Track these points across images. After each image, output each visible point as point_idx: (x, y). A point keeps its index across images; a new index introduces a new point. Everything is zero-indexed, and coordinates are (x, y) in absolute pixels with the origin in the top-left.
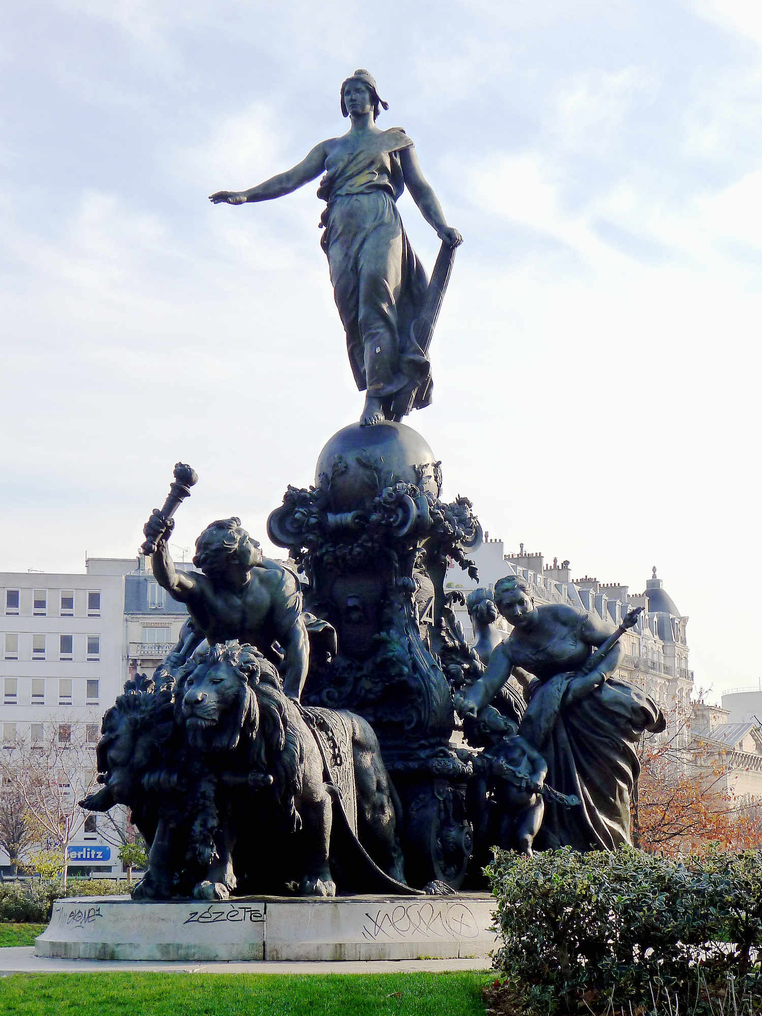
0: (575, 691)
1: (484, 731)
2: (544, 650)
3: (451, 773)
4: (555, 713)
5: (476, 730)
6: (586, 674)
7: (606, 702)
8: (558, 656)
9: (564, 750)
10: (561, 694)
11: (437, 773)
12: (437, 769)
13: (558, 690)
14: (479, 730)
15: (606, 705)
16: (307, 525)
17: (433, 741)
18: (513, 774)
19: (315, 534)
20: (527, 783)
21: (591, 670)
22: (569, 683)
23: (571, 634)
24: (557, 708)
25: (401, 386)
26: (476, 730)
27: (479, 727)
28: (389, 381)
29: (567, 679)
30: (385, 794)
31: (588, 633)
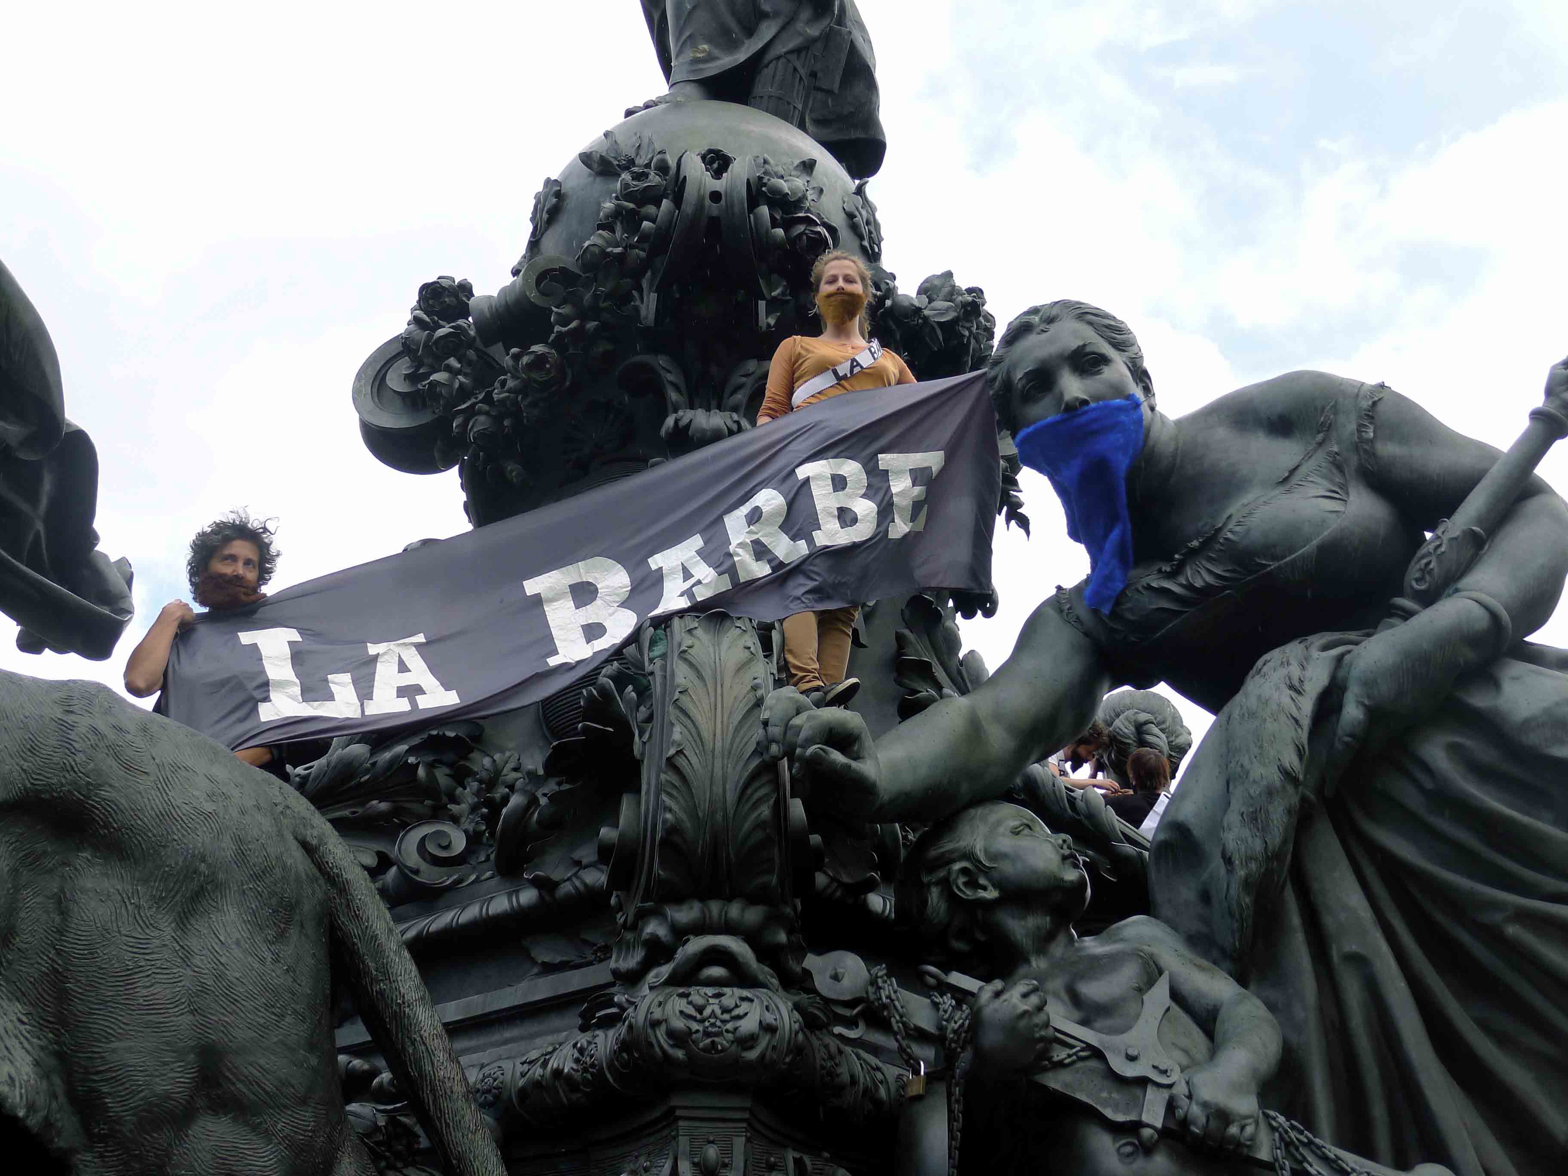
0: (1368, 683)
1: (969, 894)
2: (1209, 541)
3: (752, 1055)
4: (1288, 775)
5: (934, 895)
6: (1407, 615)
7: (1527, 724)
8: (1269, 550)
9: (1359, 961)
10: (1307, 705)
11: (679, 1054)
12: (678, 1038)
13: (1292, 687)
14: (952, 898)
15: (1533, 739)
16: (426, 345)
17: (685, 914)
18: (1093, 1064)
19: (449, 369)
20: (1171, 1106)
21: (1428, 599)
22: (1340, 659)
23: (1320, 457)
24: (1291, 759)
25: (760, 45)
26: (934, 895)
27: (946, 884)
28: (732, 45)
29: (1326, 648)
30: (267, 1135)
31: (1388, 449)
